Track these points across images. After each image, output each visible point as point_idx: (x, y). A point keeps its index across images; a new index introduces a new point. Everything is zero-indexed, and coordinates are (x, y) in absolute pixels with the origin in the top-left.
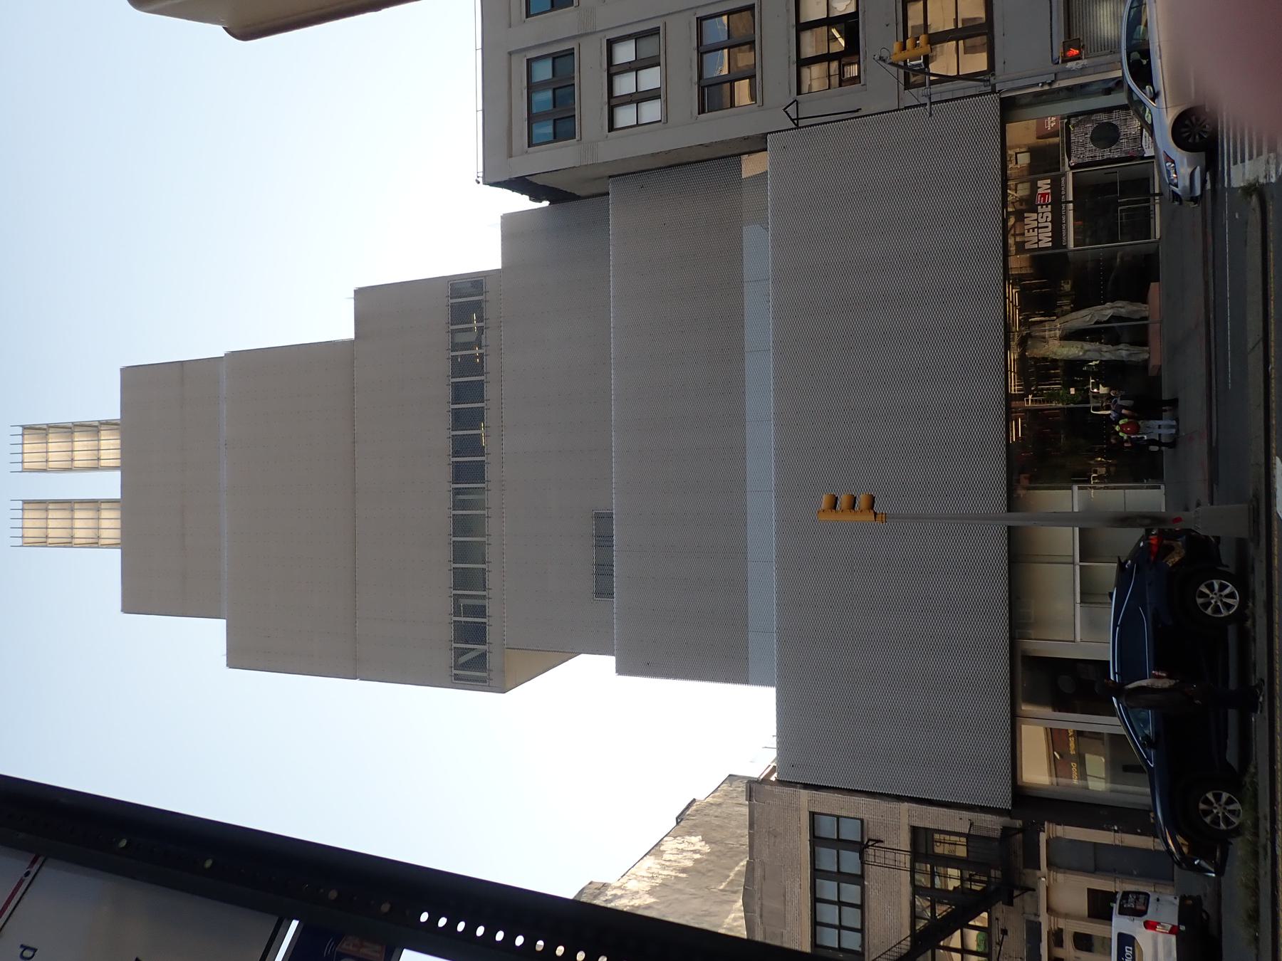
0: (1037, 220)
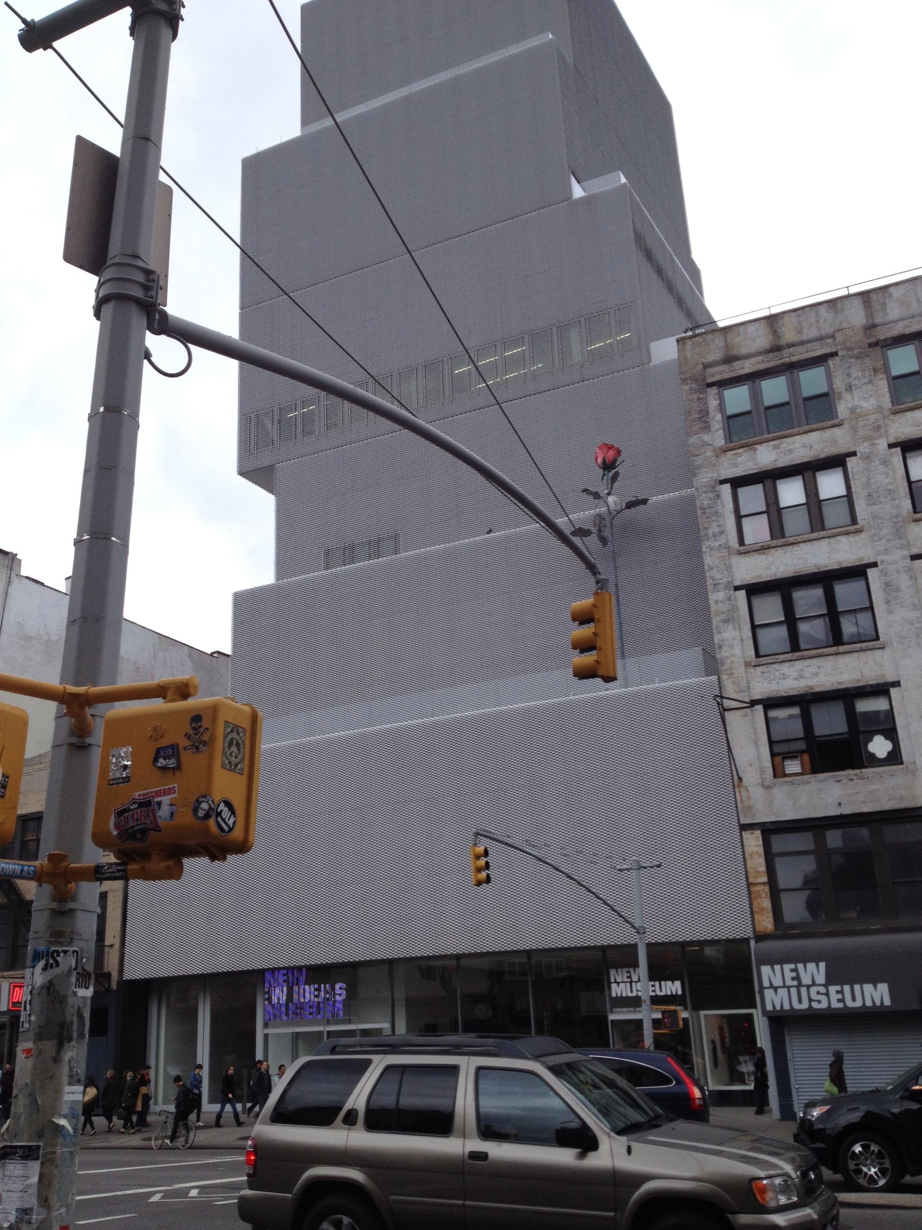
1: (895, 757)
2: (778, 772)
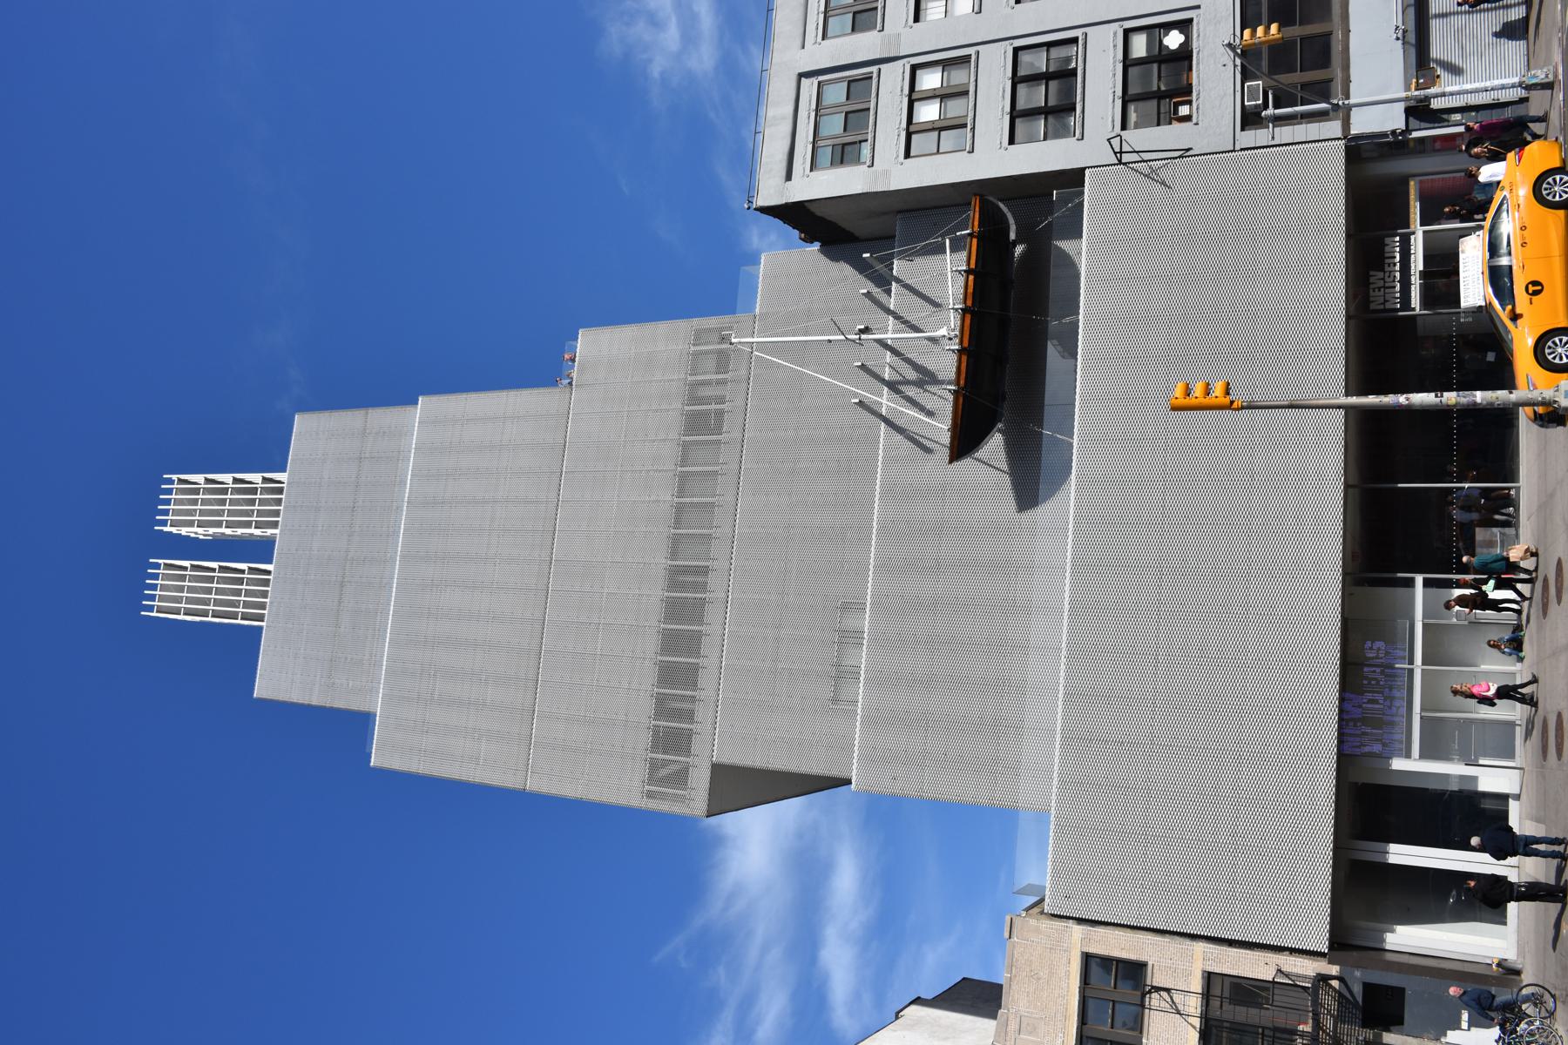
0: (1383, 279)
1: (1184, 26)
2: (1188, 118)
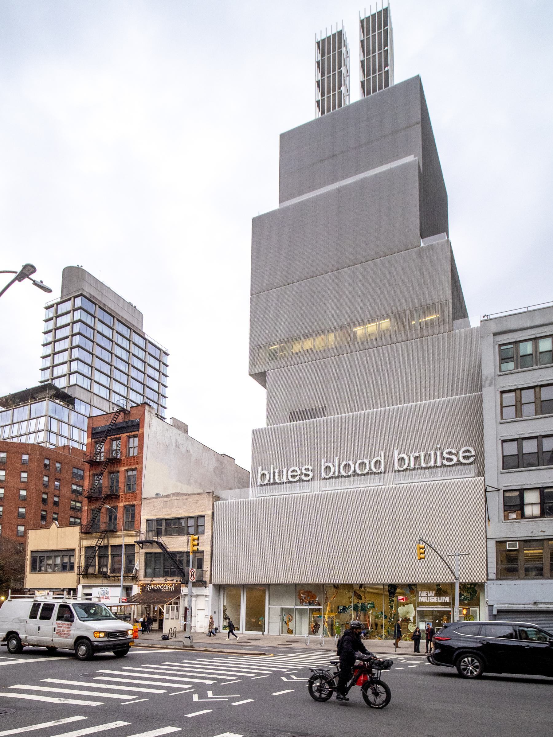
0: (431, 596)
